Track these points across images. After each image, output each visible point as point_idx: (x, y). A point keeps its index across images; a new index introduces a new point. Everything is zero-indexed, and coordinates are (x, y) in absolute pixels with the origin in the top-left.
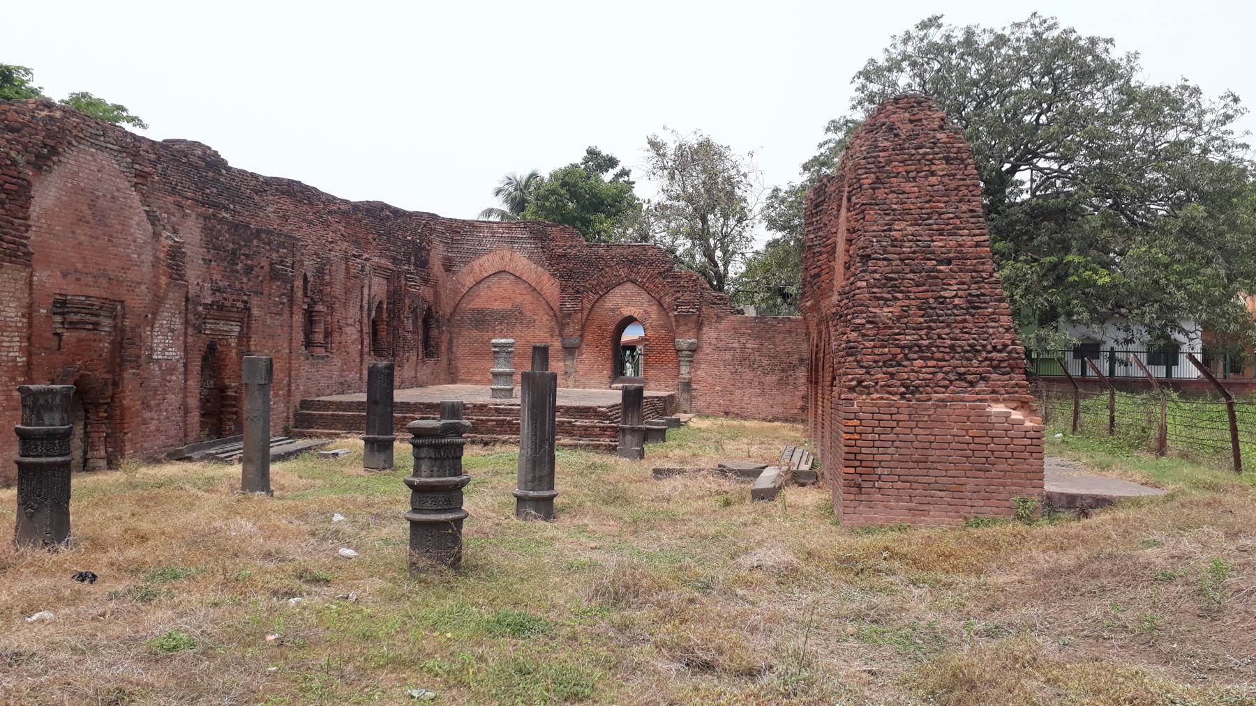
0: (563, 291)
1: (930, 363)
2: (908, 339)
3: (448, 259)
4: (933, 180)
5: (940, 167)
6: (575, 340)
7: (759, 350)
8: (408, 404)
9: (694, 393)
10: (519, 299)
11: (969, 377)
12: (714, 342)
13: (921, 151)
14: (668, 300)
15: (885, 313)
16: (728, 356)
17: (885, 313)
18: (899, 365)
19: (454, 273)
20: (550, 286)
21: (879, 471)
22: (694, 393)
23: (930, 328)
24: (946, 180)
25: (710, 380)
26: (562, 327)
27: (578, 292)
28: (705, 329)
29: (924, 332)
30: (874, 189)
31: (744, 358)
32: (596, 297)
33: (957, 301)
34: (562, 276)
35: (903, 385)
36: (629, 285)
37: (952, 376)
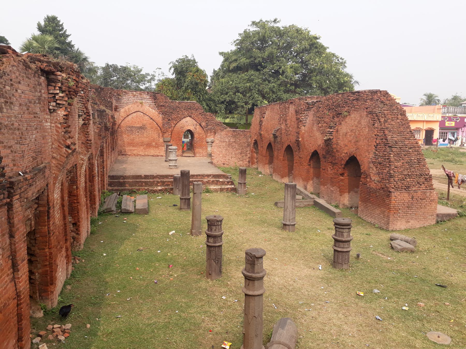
0: (163, 119)
1: (411, 179)
2: (406, 173)
3: (116, 106)
4: (398, 121)
5: (400, 117)
6: (169, 139)
7: (235, 142)
8: (153, 175)
9: (213, 158)
10: (145, 122)
11: (421, 183)
12: (219, 139)
13: (395, 111)
14: (203, 124)
15: (399, 164)
16: (224, 144)
17: (399, 164)
18: (404, 180)
19: (118, 111)
20: (159, 118)
21: (399, 211)
22: (213, 158)
23: (410, 169)
24: (401, 121)
25: (218, 153)
26: (164, 133)
27: (169, 120)
28: (216, 134)
29: (409, 170)
30: (384, 123)
31: (230, 144)
32: (176, 122)
33: (415, 161)
34: (163, 114)
35: (405, 186)
36: (189, 117)
37: (416, 183)
